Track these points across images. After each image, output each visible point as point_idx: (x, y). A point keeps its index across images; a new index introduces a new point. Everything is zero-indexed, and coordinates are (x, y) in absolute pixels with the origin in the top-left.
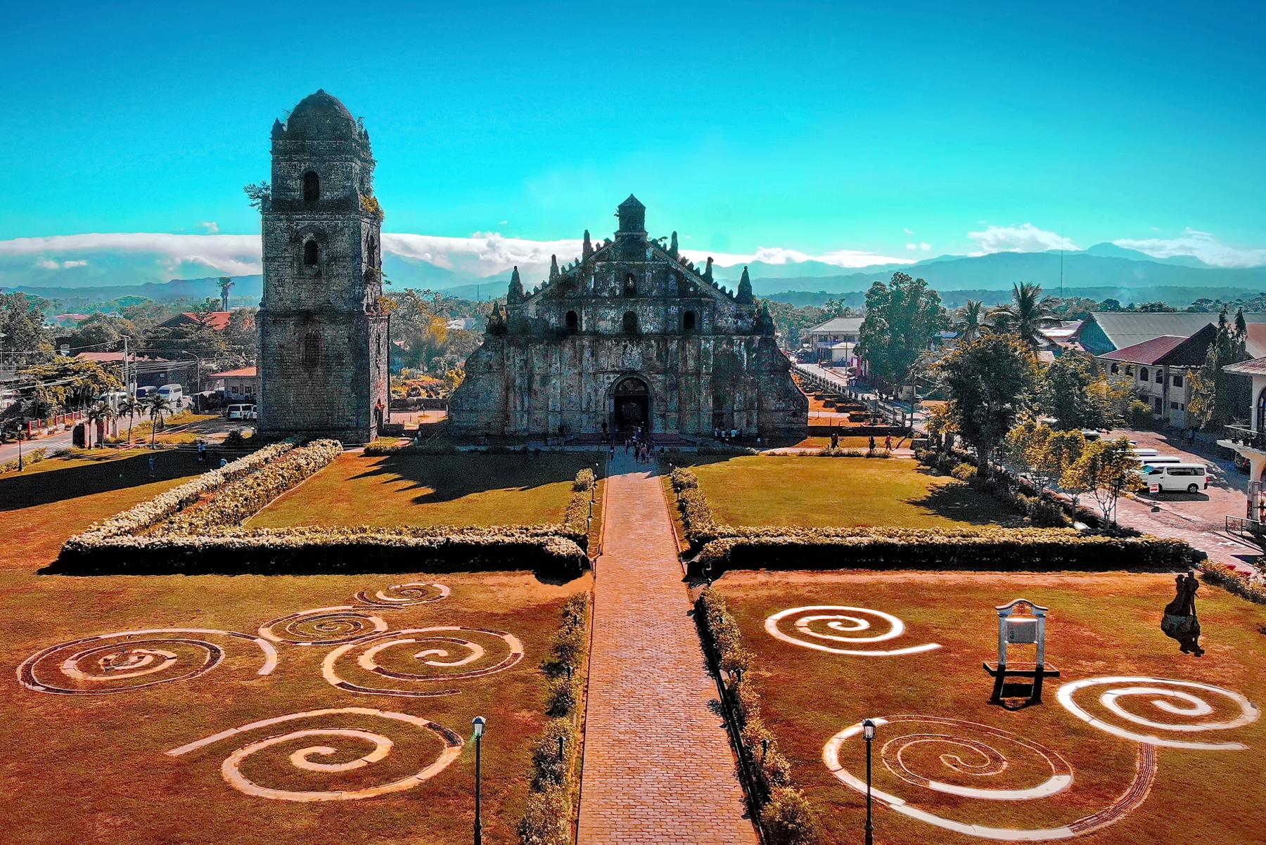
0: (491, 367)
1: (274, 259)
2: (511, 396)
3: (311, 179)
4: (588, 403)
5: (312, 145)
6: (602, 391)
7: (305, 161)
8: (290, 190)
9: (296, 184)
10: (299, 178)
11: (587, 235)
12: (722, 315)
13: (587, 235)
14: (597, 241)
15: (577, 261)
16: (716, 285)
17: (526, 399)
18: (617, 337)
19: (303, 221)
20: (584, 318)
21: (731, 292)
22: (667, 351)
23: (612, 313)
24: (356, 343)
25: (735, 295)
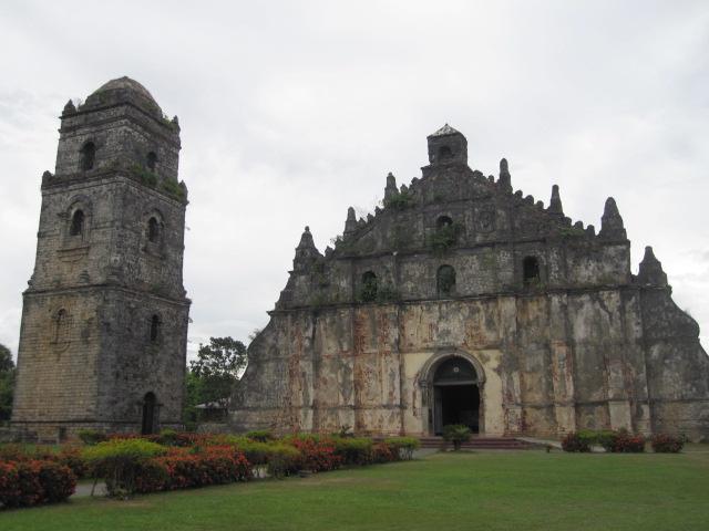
0: (277, 352)
3: (89, 149)
4: (391, 394)
8: (70, 164)
9: (76, 157)
10: (80, 151)
11: (391, 179)
13: (391, 179)
14: (404, 180)
15: (377, 209)
16: (569, 220)
17: (311, 390)
21: (591, 228)
22: (499, 315)
24: (103, 317)
25: (597, 231)
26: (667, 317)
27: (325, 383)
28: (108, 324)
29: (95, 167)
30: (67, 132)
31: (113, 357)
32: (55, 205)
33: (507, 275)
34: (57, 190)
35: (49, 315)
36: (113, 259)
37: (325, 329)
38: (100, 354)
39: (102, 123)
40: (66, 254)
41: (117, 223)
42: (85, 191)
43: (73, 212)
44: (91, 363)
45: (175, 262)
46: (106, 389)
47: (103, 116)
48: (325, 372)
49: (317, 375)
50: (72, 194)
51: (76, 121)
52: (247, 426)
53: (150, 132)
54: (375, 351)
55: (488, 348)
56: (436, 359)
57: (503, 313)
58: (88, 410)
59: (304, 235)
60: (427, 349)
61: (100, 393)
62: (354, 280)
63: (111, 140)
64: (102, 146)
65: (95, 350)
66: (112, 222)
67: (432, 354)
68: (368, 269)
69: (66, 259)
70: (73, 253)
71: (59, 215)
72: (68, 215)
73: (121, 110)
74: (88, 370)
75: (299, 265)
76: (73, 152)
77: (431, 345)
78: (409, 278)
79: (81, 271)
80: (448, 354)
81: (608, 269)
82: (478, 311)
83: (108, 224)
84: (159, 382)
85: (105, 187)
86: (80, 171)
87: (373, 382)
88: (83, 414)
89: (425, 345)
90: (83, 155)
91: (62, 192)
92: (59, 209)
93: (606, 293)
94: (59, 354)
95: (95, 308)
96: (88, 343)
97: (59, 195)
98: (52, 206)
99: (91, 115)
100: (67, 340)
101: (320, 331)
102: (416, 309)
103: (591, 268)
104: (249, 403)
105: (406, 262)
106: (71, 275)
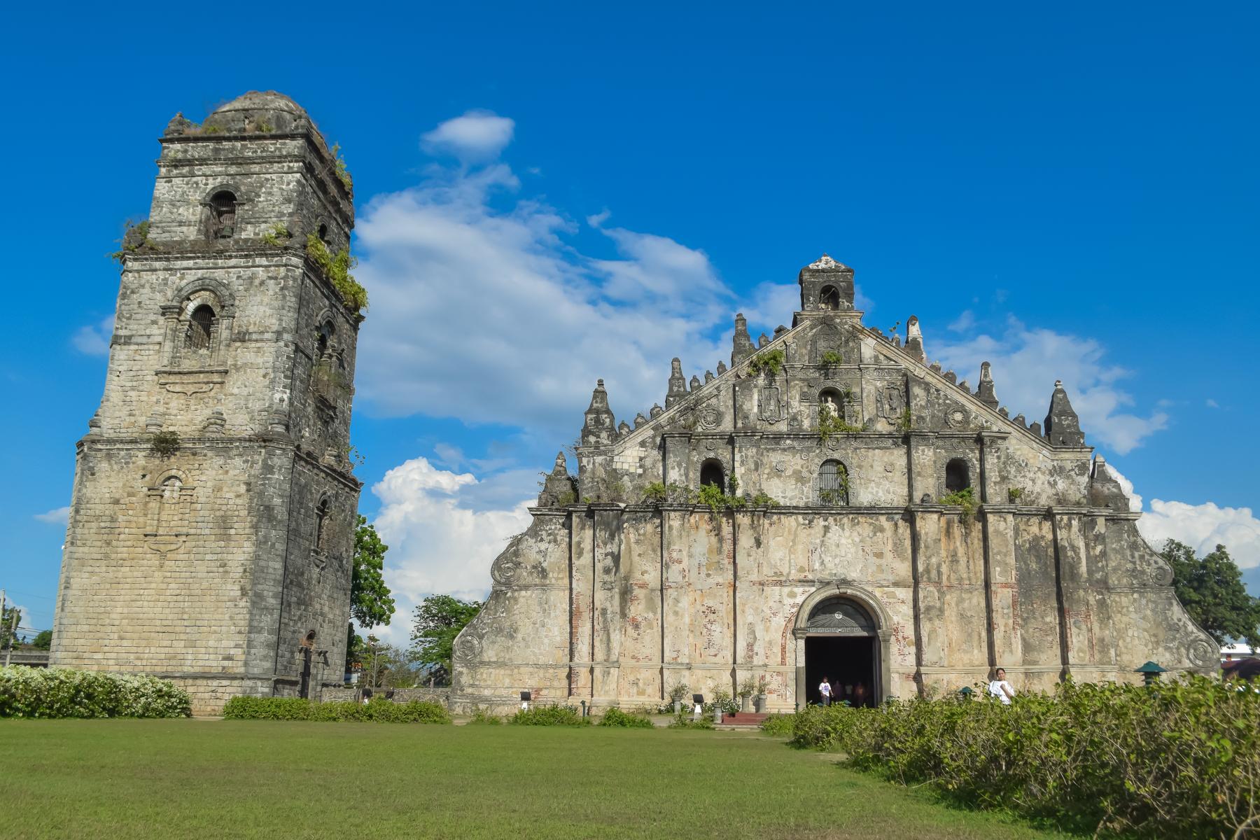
1: (128, 340)
2: (584, 629)
3: (223, 200)
4: (750, 647)
5: (234, 149)
6: (779, 622)
7: (215, 176)
8: (181, 224)
9: (194, 213)
12: (1021, 467)
17: (616, 637)
18: (810, 512)
19: (189, 273)
20: (739, 471)
22: (915, 537)
23: (794, 462)
24: (261, 494)
26: (1133, 557)
27: (637, 627)
28: (269, 508)
29: (236, 236)
30: (176, 167)
31: (278, 565)
32: (153, 289)
33: (930, 483)
34: (157, 264)
35: (141, 487)
36: (277, 396)
37: (637, 542)
38: (257, 558)
39: (250, 161)
40: (172, 378)
41: (286, 336)
42: (219, 274)
43: (191, 306)
44: (237, 572)
45: (343, 412)
46: (268, 621)
47: (251, 149)
48: (636, 610)
49: (624, 615)
50: (191, 276)
51: (195, 150)
52: (487, 692)
53: (325, 192)
54: (721, 581)
55: (896, 584)
56: (818, 598)
57: (923, 537)
58: (229, 658)
59: (596, 391)
60: (804, 582)
61: (252, 629)
62: (687, 469)
63: (270, 194)
64: (250, 200)
65: (241, 552)
66: (279, 334)
67: (814, 589)
68: (712, 455)
69: (178, 388)
70: (192, 378)
71: (165, 311)
72: (181, 310)
73: (294, 146)
74: (229, 587)
75: (592, 439)
76: (188, 203)
77: (810, 577)
78: (778, 472)
79: (208, 412)
80: (837, 591)
81: (1061, 485)
82: (882, 530)
83: (267, 336)
84: (322, 614)
85: (261, 268)
86: (202, 237)
87: (716, 628)
88: (216, 665)
89: (802, 576)
90: (207, 211)
91: (165, 269)
92: (160, 300)
93: (1065, 518)
94: (163, 555)
95: (245, 478)
96: (227, 538)
97: (161, 275)
98: (147, 290)
99: (226, 144)
100: (185, 530)
101: (628, 544)
102: (790, 522)
103: (1039, 482)
104: (490, 654)
105: (774, 450)
106: (185, 419)
